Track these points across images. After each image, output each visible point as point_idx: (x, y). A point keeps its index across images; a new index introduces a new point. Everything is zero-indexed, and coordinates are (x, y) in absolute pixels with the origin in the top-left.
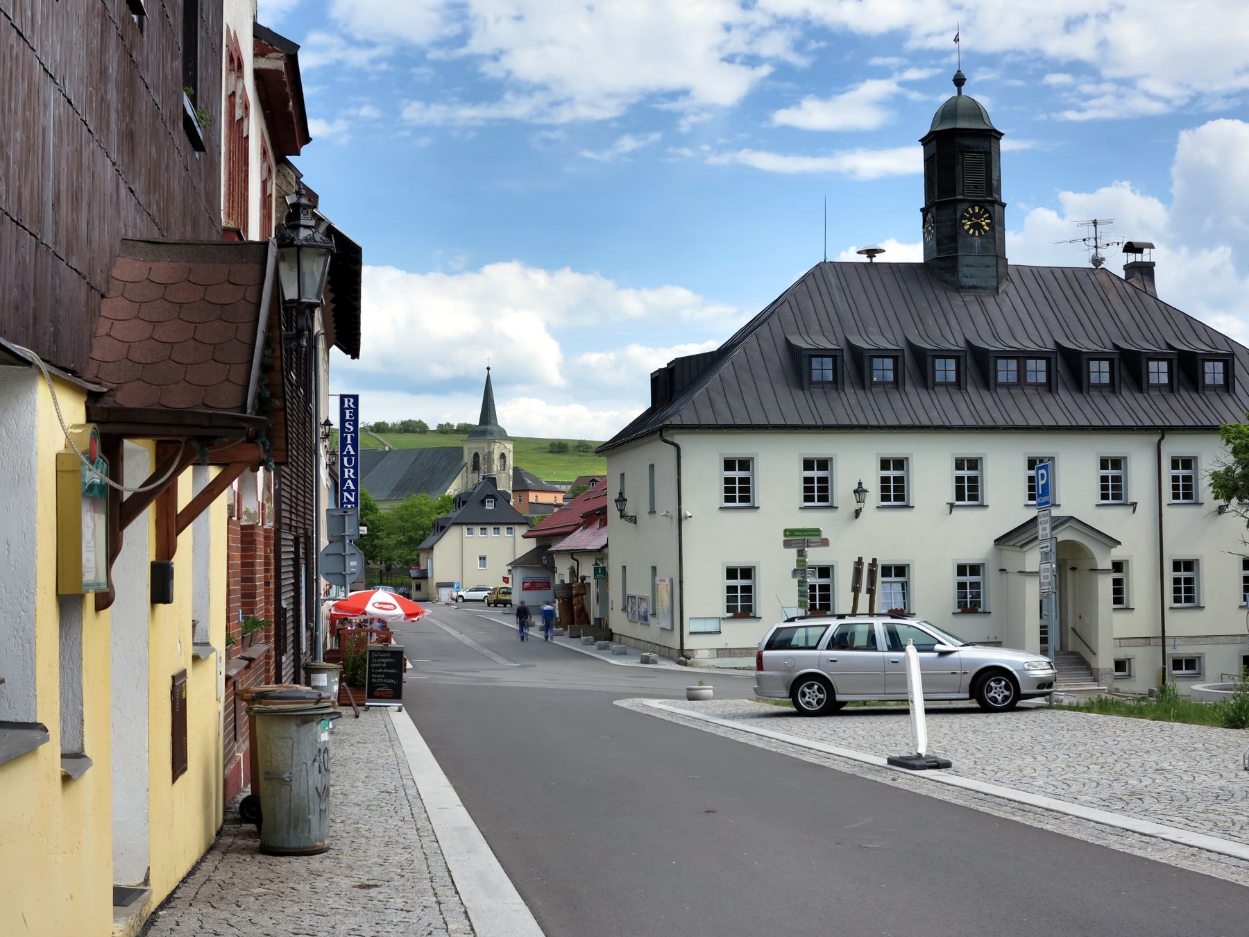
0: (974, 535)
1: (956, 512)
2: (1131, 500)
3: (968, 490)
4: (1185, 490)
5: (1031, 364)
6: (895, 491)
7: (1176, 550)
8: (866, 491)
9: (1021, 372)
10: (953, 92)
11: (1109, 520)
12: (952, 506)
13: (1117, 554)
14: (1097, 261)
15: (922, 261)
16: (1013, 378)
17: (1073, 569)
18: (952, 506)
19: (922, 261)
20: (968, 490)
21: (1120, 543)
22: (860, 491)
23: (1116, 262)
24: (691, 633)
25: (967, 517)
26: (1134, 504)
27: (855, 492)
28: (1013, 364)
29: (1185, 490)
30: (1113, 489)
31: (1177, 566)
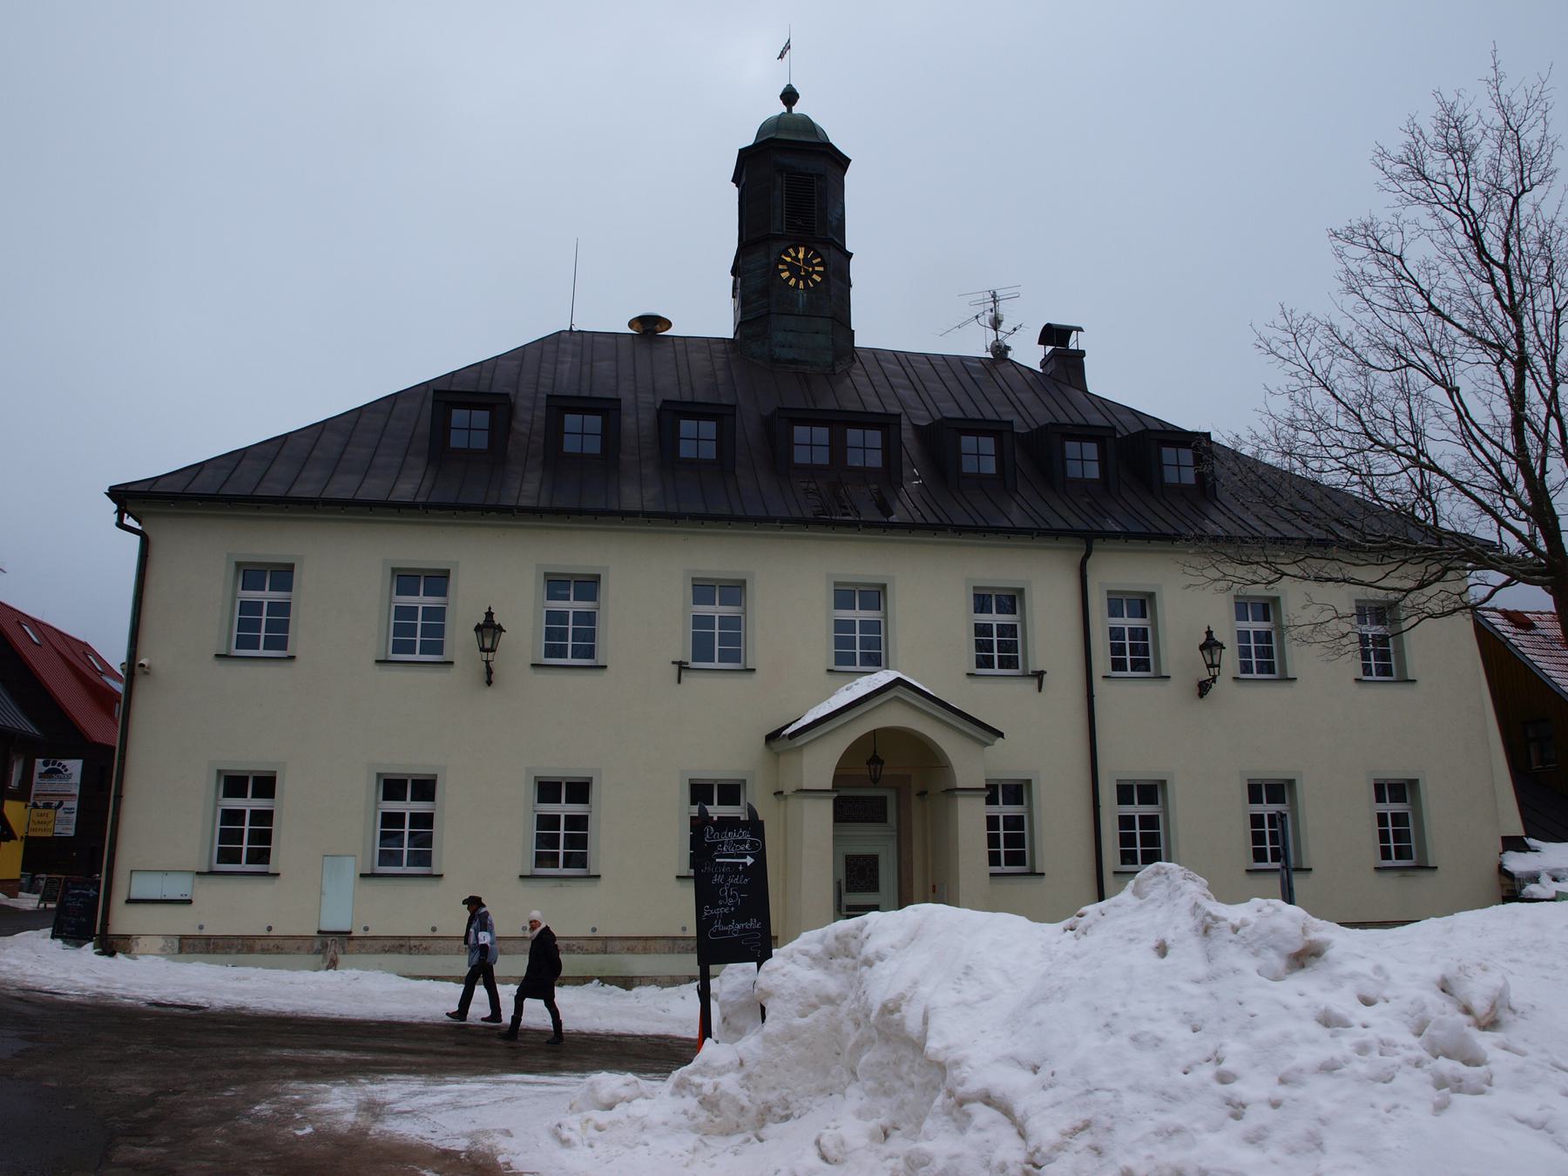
0: (717, 730)
1: (694, 683)
2: (1032, 668)
3: (717, 644)
4: (1135, 655)
5: (854, 435)
6: (572, 641)
7: (1125, 759)
8: (500, 629)
9: (838, 447)
10: (784, 109)
11: (992, 698)
12: (682, 666)
13: (1001, 762)
14: (1000, 351)
15: (726, 330)
16: (822, 457)
17: (922, 794)
18: (682, 666)
19: (726, 330)
20: (717, 644)
21: (1001, 735)
22: (489, 629)
23: (1029, 354)
24: (129, 901)
25: (709, 687)
26: (1039, 675)
27: (478, 628)
28: (822, 434)
29: (1135, 655)
30: (998, 650)
31: (1124, 793)
